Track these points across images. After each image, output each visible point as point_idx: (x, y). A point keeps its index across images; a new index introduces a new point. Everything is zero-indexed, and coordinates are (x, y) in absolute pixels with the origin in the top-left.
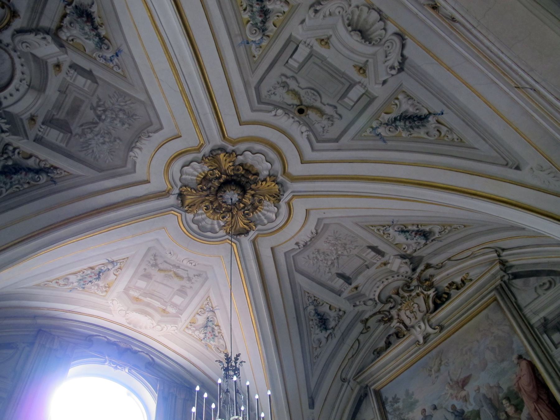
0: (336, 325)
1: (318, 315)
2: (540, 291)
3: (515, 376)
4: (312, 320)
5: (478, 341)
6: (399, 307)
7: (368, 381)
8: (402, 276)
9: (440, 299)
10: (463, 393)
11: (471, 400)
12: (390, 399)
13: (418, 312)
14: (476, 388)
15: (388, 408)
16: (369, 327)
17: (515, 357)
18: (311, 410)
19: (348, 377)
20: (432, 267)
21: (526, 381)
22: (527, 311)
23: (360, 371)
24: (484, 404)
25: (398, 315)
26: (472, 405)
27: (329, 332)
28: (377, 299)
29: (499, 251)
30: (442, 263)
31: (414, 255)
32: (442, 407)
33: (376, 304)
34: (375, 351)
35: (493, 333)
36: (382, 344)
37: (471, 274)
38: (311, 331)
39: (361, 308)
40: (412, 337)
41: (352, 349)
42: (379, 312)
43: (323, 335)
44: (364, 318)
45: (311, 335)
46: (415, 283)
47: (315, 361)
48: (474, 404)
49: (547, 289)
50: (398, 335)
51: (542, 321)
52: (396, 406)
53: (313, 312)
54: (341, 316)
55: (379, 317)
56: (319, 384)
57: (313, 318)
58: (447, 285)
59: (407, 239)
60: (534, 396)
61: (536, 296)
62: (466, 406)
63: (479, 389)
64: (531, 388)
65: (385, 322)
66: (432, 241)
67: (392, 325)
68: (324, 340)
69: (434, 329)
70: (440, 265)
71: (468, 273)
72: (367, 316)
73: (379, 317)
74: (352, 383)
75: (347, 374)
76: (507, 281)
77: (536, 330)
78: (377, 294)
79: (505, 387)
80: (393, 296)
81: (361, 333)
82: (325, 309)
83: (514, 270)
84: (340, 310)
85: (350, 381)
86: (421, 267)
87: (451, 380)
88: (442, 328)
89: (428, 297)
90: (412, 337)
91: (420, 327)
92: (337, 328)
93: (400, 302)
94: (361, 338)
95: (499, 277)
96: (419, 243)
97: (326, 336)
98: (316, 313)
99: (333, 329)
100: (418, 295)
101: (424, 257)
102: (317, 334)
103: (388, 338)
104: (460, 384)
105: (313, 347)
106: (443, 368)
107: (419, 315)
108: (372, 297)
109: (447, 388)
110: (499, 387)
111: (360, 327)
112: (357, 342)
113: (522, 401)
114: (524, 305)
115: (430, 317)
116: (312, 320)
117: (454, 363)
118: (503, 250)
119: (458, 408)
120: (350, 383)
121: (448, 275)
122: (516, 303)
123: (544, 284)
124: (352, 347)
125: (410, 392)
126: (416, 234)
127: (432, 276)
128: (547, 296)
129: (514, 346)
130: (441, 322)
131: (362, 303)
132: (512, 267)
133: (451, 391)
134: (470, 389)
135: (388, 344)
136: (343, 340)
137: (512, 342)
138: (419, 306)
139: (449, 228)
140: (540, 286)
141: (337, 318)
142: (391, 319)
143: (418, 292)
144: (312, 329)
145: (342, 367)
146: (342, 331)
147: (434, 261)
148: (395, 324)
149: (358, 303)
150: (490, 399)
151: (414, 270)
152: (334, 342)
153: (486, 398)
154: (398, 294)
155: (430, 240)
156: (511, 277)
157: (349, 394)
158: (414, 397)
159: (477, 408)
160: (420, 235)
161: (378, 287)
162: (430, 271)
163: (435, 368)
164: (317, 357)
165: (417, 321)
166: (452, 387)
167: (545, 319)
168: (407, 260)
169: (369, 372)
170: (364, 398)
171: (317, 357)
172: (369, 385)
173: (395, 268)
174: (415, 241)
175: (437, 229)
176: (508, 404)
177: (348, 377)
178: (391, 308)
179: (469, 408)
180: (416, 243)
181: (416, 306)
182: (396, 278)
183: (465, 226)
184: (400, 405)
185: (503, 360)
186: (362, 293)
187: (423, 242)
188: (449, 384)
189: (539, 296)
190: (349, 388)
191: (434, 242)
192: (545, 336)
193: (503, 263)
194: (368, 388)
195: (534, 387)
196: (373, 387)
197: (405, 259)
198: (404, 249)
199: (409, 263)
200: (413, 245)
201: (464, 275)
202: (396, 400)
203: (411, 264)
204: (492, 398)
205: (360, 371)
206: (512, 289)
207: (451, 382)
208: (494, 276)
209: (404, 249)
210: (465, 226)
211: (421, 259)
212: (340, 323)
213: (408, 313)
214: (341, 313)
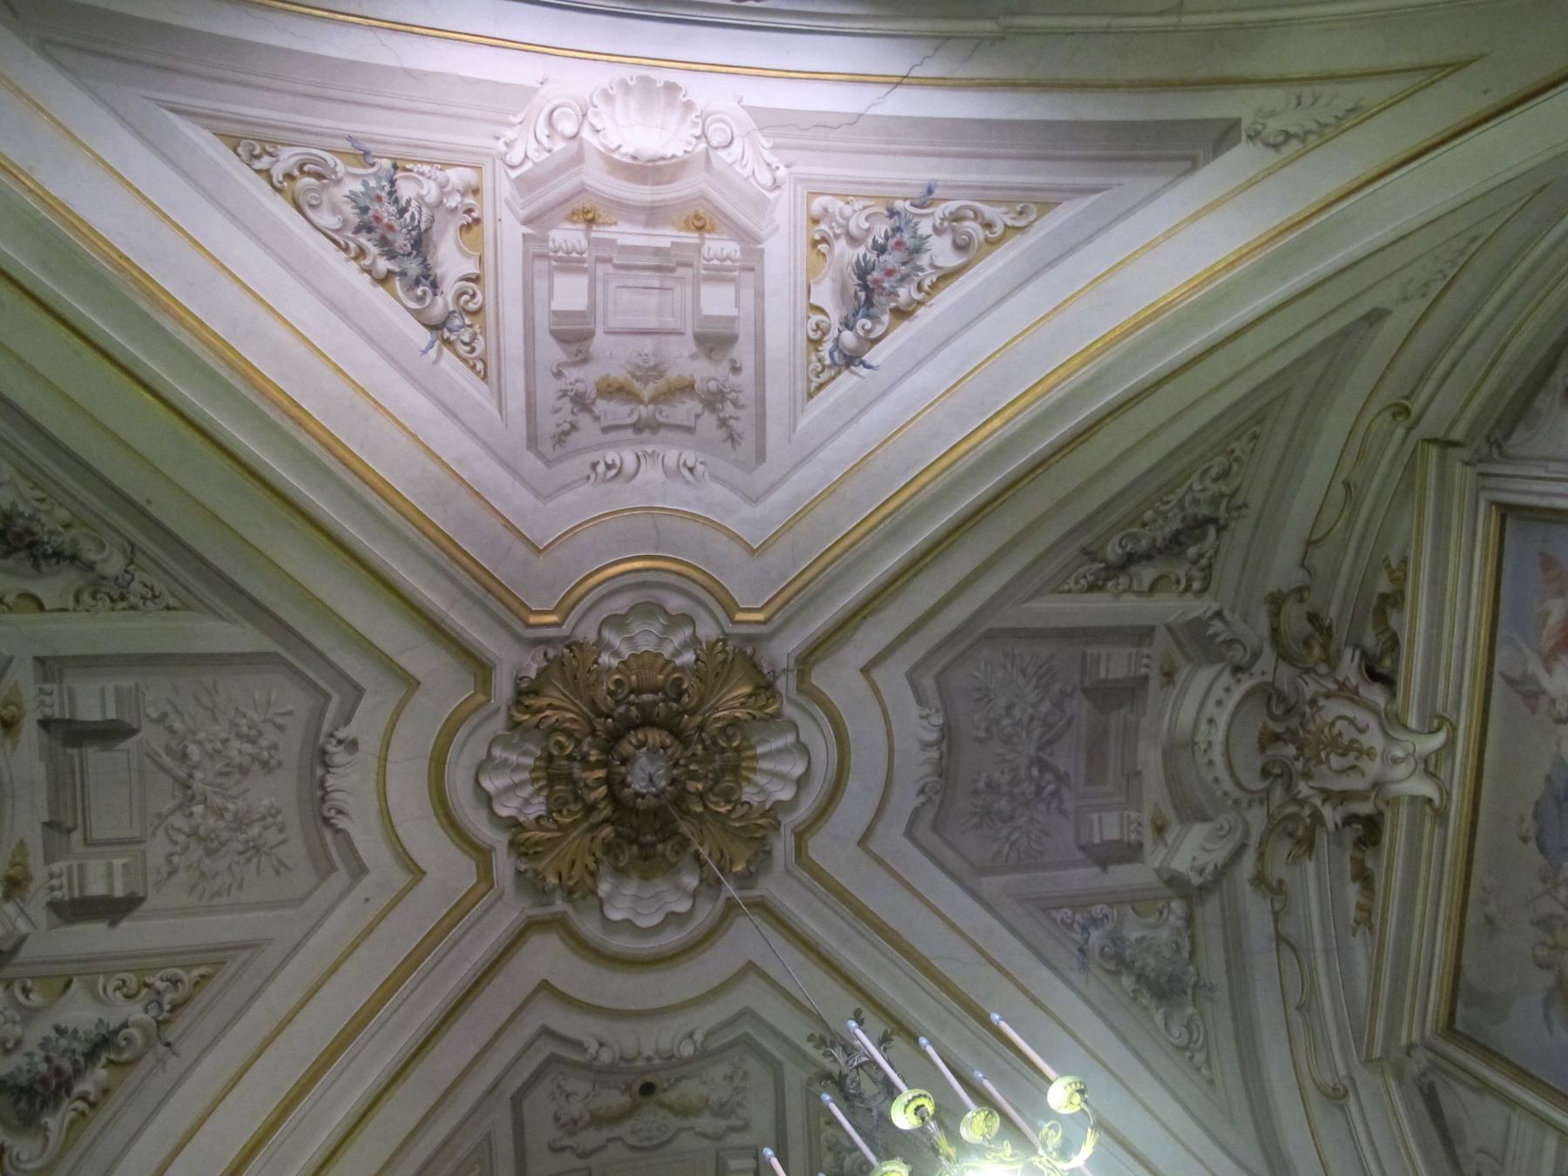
1: (58, 555)
4: (67, 526)
38: (35, 486)
45: (19, 471)
53: (90, 553)
57: (67, 536)
59: (61, 1031)
82: (53, 587)
98: (74, 558)
116: (67, 526)
126: (58, 1072)
144: (38, 494)
160: (44, 1081)
174: (31, 1045)
198: (26, 991)
200: (18, 1030)
209: (26, 991)
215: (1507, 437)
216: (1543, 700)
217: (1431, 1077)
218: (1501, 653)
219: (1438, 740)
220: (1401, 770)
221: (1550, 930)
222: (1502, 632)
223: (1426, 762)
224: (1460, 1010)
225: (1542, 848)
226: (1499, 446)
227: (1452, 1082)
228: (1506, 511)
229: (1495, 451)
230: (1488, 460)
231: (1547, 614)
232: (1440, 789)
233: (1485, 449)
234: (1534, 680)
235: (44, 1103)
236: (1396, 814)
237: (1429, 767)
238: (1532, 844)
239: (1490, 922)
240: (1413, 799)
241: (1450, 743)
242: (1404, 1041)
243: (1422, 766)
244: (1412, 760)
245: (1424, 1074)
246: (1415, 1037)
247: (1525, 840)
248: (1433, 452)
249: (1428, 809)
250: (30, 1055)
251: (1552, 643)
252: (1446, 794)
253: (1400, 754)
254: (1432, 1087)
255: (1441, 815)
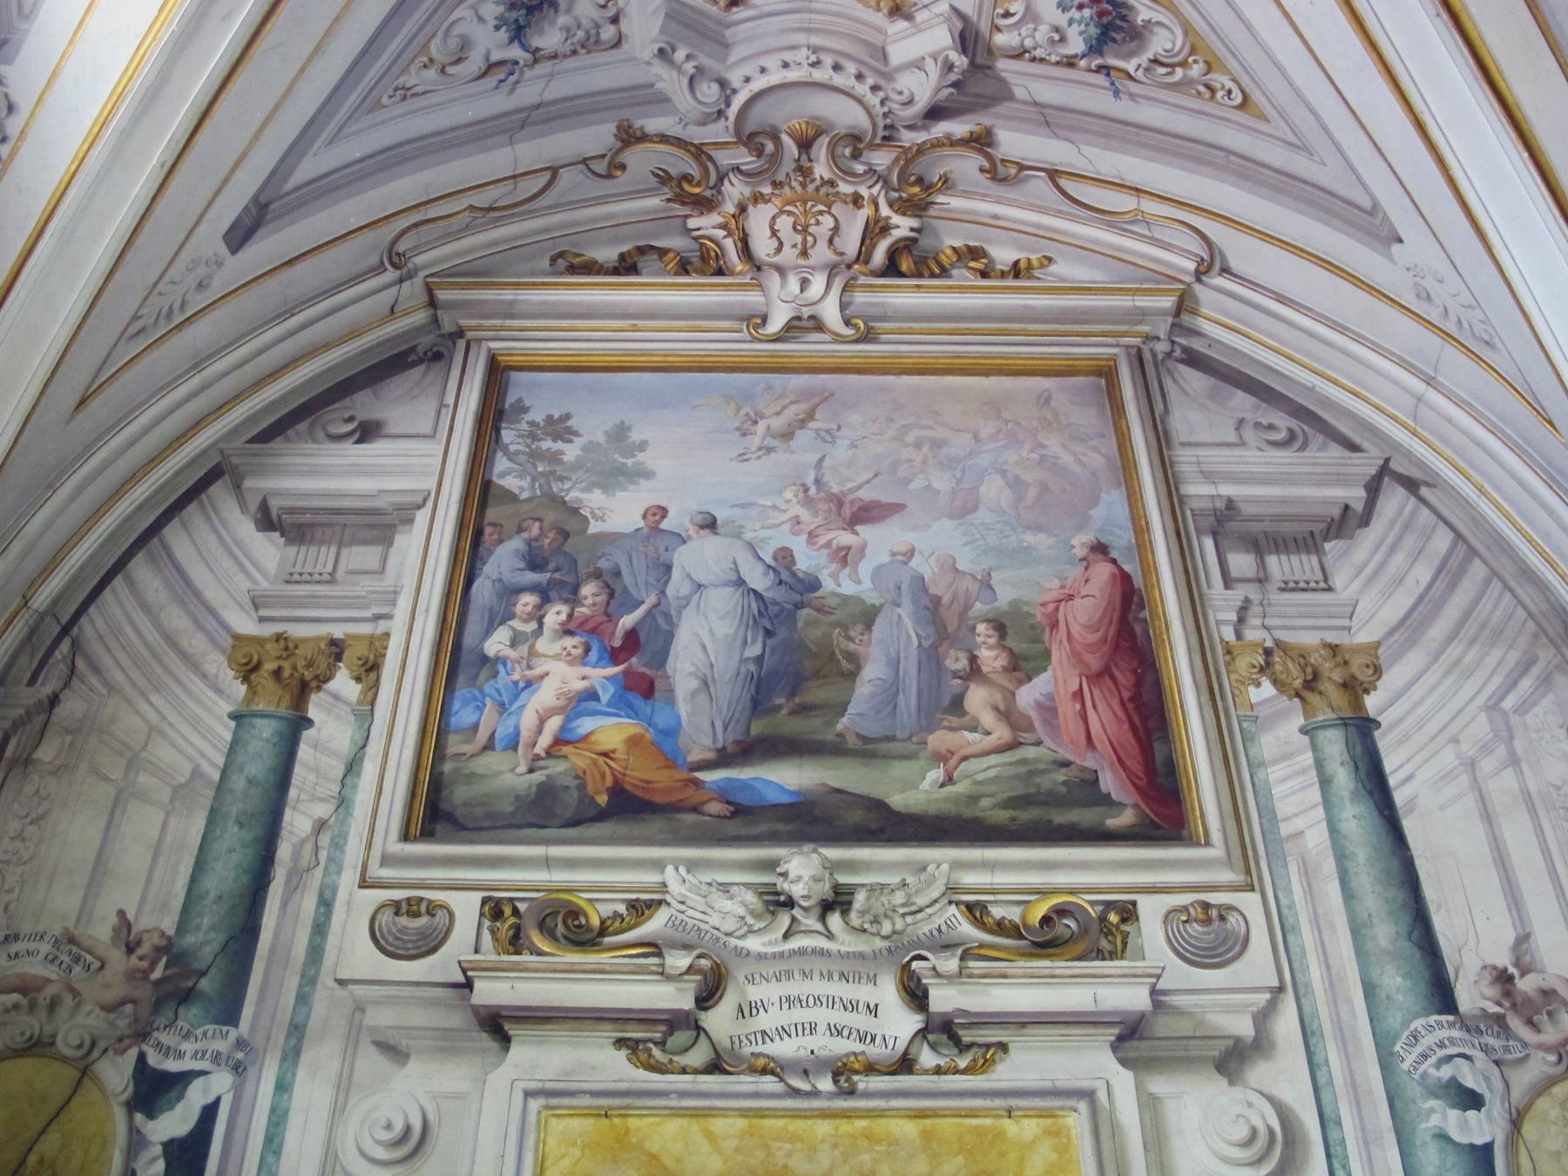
0: (554, 56)
2: (1249, 434)
3: (1056, 583)
5: (976, 438)
6: (767, 190)
7: (474, 322)
8: (882, 103)
9: (910, 261)
10: (846, 538)
11: (865, 569)
12: (537, 415)
13: (822, 244)
14: (903, 549)
15: (507, 435)
16: (623, 167)
17: (1081, 541)
18: (224, 250)
19: (419, 260)
20: (989, 157)
21: (1086, 612)
22: (1185, 459)
23: (476, 273)
24: (906, 601)
25: (742, 209)
26: (859, 582)
27: (516, 52)
28: (738, 102)
29: (1212, 263)
30: (1022, 168)
31: (1003, 65)
32: (738, 535)
33: (720, 113)
34: (561, 255)
35: (1043, 446)
36: (607, 254)
37: (1053, 268)
39: (669, 81)
40: (753, 298)
41: (509, 185)
42: (699, 152)
43: (490, 42)
44: (638, 123)
46: (881, 159)
47: (385, 100)
48: (867, 583)
49: (1275, 444)
50: (703, 263)
51: (1220, 505)
52: (547, 444)
54: (597, 42)
55: (684, 164)
56: (326, 188)
58: (958, 244)
60: (1095, 662)
61: (1232, 437)
62: (835, 576)
63: (911, 553)
64: (1093, 637)
65: (681, 198)
66: (1099, 69)
67: (692, 223)
68: (475, 63)
69: (847, 323)
70: (1013, 171)
71: (1050, 260)
72: (653, 125)
73: (684, 164)
74: (413, 290)
75: (419, 249)
76: (1160, 357)
77: (1188, 513)
78: (759, 83)
79: (1005, 595)
80: (784, 137)
81: (585, 161)
83: (1197, 345)
84: (615, 20)
85: (410, 276)
86: (957, 128)
87: (817, 481)
88: (867, 337)
89: (886, 229)
90: (753, 298)
91: (804, 284)
92: (543, 68)
93: (780, 177)
94: (567, 177)
95: (1145, 328)
96: (1063, 40)
97: (496, 56)
99: (536, 56)
100: (857, 200)
101: (1008, 96)
102: (481, 19)
103: (642, 251)
104: (847, 512)
105: (426, 45)
106: (803, 437)
107: (822, 253)
108: (735, 78)
109: (788, 494)
110: (986, 584)
111: (597, 137)
112: (547, 176)
113: (1047, 654)
114: (1184, 439)
115: (862, 280)
117: (853, 446)
118: (1226, 270)
119: (803, 564)
120: (406, 285)
121: (995, 217)
122: (1163, 422)
123: (1271, 427)
124: (514, 177)
125: (635, 436)
127: (946, 183)
128: (1258, 458)
129: (1097, 513)
130: (883, 318)
131: (689, 68)
132: (1196, 333)
133: (797, 510)
134: (880, 541)
135: (626, 266)
136: (522, 127)
137: (1094, 502)
138: (836, 230)
139: (1196, 71)
140: (1258, 425)
141: (580, 34)
142: (705, 205)
143: (864, 192)
145: (433, 212)
146: (547, 97)
147: (1013, 143)
148: (706, 224)
149: (680, 55)
150: (936, 601)
151: (935, 113)
152: (494, 101)
153: (925, 589)
154: (805, 145)
155: (1099, 61)
156: (1178, 353)
157: (375, 312)
158: (640, 457)
159: (872, 598)
160: (1101, 14)
161: (786, 65)
162: (967, 166)
163: (778, 423)
164: (406, 93)
165: (802, 262)
166: (808, 502)
167: (1230, 504)
168: (960, 61)
169: (508, 295)
170: (421, 361)
171: (406, 93)
172: (470, 335)
173: (899, 53)
174: (1061, 19)
175: (1161, 43)
176: (992, 641)
177: (419, 260)
178: (737, 169)
179: (839, 584)
180: (1057, 29)
181: (828, 222)
182: (862, 89)
183: (1245, 104)
184: (571, 452)
185: (1037, 528)
186: (728, 33)
187: (1076, 45)
188: (806, 490)
189: (1242, 444)
190: (387, 297)
191: (1100, 79)
192: (1209, 543)
193: (1185, 304)
194: (461, 344)
195: (1104, 641)
196: (493, 345)
197: (964, 51)
199: (953, 77)
200: (1044, 29)
201: (1034, 257)
202: (559, 428)
203: (954, 85)
204: (945, 600)
205: (476, 273)
206: (1168, 382)
207: (813, 491)
208: (1143, 314)
209: (1007, 15)
210: (1245, 104)
211: (1003, 94)
212: (570, 63)
213: (785, 224)
214: (608, 33)
235: (1124, 18)
250: (1071, 22)
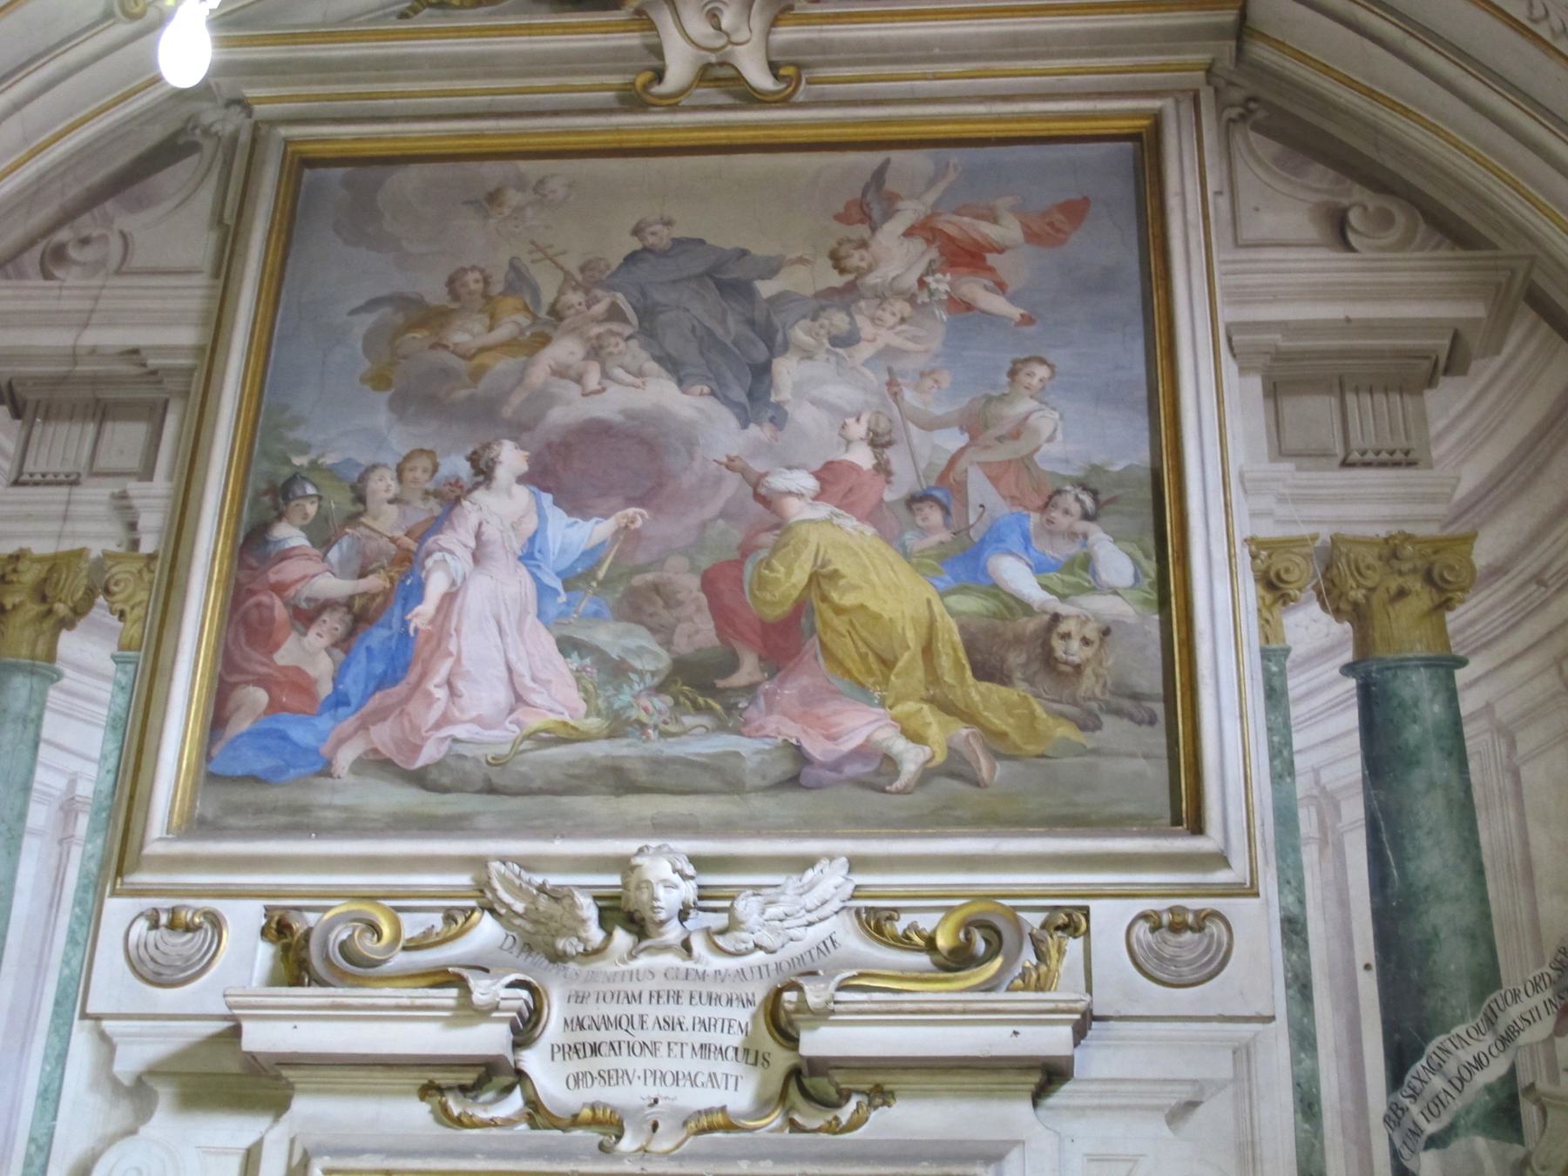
215: (1257, 128)
216: (862, 231)
217: (208, 145)
218: (919, 161)
219: (760, 79)
220: (698, 27)
221: (510, 289)
222: (955, 156)
223: (722, 64)
224: (338, 172)
225: (632, 258)
226: (1243, 117)
227: (213, 181)
228: (1145, 148)
229: (1234, 112)
230: (1221, 105)
231: (995, 220)
232: (683, 92)
233: (1236, 95)
234: (888, 215)
236: (623, 27)
237: (718, 76)
238: (636, 245)
239: (494, 198)
240: (657, 51)
241: (751, 98)
242: (250, 93)
243: (713, 58)
244: (719, 43)
245: (206, 132)
246: (261, 110)
247: (637, 231)
248: (1228, 17)
249: (641, 79)
251: (951, 230)
252: (672, 103)
253: (726, 22)
254: (194, 147)
255: (633, 100)
